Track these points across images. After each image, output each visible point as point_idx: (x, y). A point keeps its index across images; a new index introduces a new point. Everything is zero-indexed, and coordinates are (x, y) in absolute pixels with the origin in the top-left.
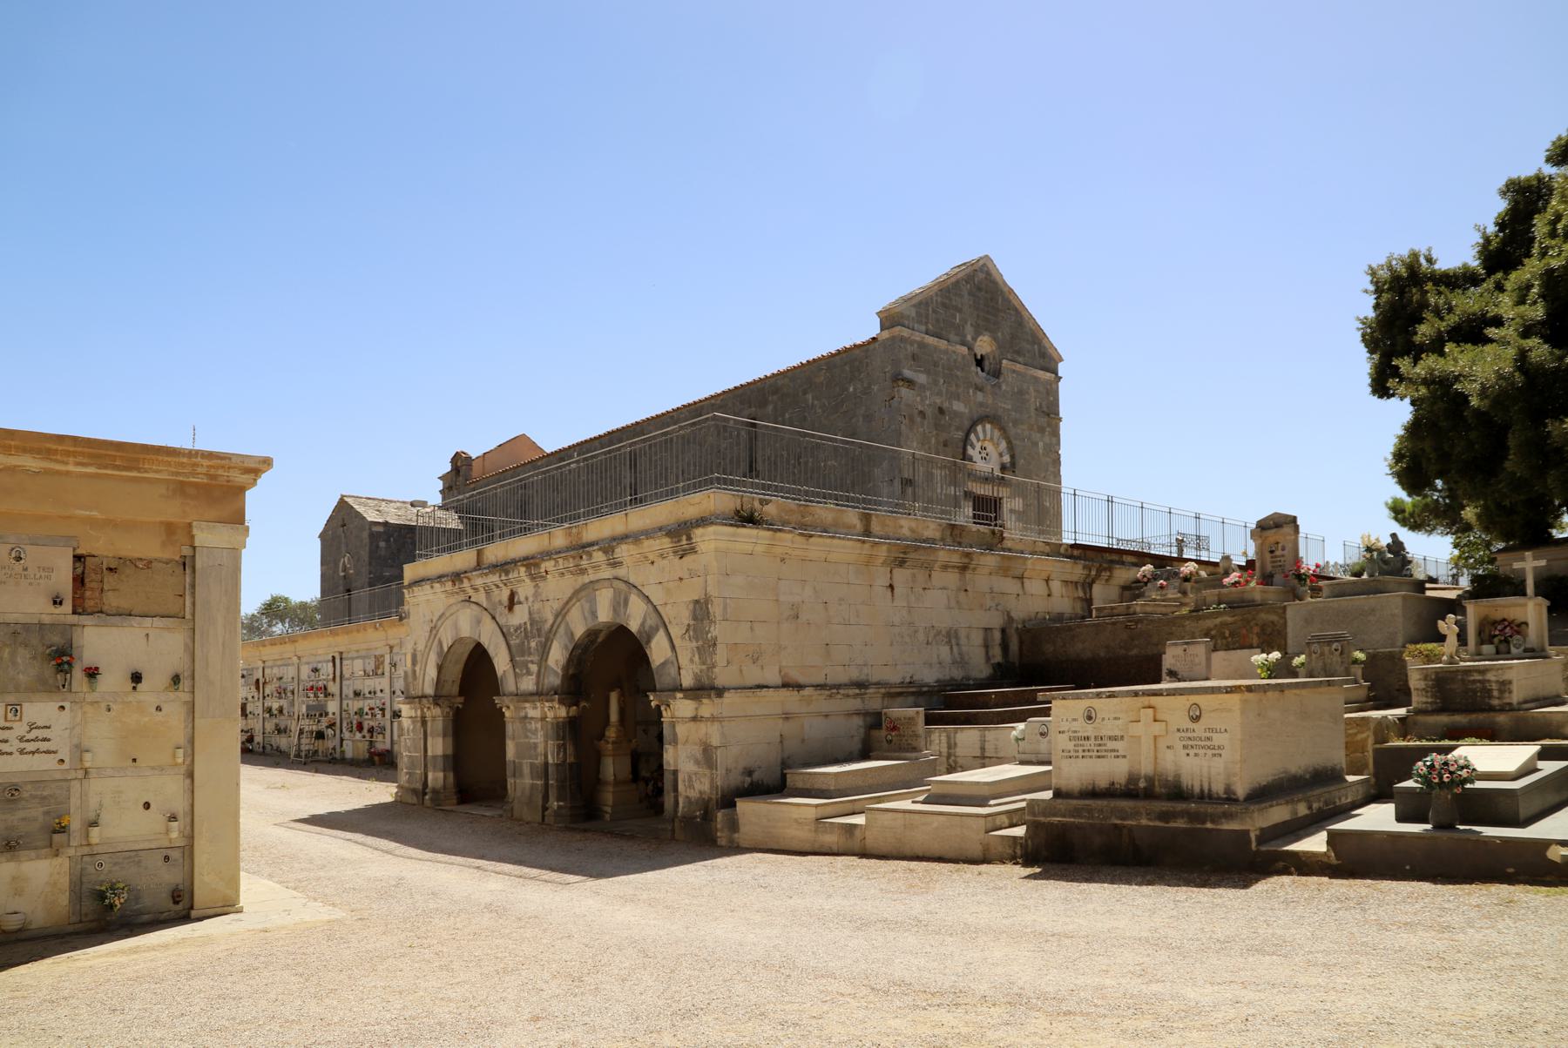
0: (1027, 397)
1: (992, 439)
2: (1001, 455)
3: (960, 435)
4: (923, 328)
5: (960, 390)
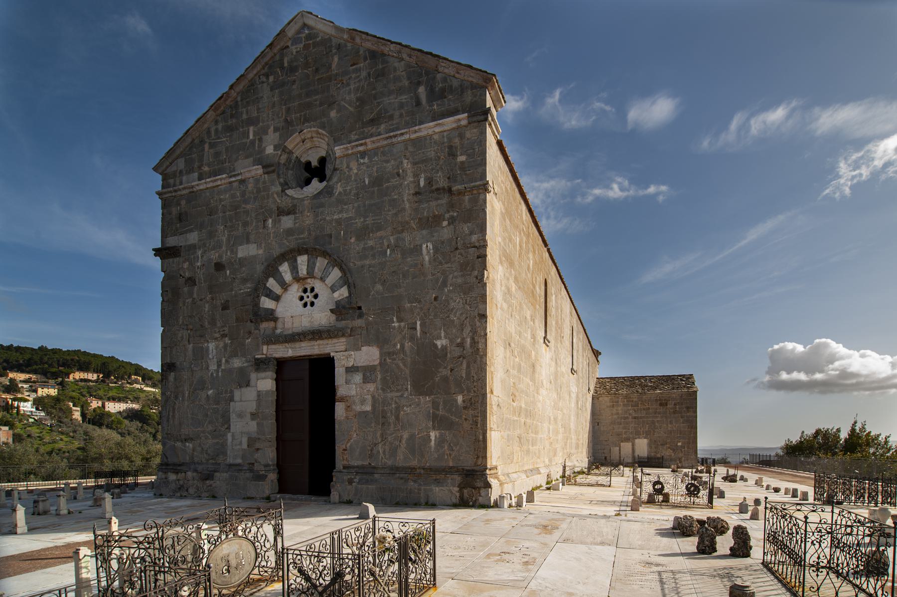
1: (311, 274)
3: (248, 287)
4: (196, 175)
5: (249, 229)
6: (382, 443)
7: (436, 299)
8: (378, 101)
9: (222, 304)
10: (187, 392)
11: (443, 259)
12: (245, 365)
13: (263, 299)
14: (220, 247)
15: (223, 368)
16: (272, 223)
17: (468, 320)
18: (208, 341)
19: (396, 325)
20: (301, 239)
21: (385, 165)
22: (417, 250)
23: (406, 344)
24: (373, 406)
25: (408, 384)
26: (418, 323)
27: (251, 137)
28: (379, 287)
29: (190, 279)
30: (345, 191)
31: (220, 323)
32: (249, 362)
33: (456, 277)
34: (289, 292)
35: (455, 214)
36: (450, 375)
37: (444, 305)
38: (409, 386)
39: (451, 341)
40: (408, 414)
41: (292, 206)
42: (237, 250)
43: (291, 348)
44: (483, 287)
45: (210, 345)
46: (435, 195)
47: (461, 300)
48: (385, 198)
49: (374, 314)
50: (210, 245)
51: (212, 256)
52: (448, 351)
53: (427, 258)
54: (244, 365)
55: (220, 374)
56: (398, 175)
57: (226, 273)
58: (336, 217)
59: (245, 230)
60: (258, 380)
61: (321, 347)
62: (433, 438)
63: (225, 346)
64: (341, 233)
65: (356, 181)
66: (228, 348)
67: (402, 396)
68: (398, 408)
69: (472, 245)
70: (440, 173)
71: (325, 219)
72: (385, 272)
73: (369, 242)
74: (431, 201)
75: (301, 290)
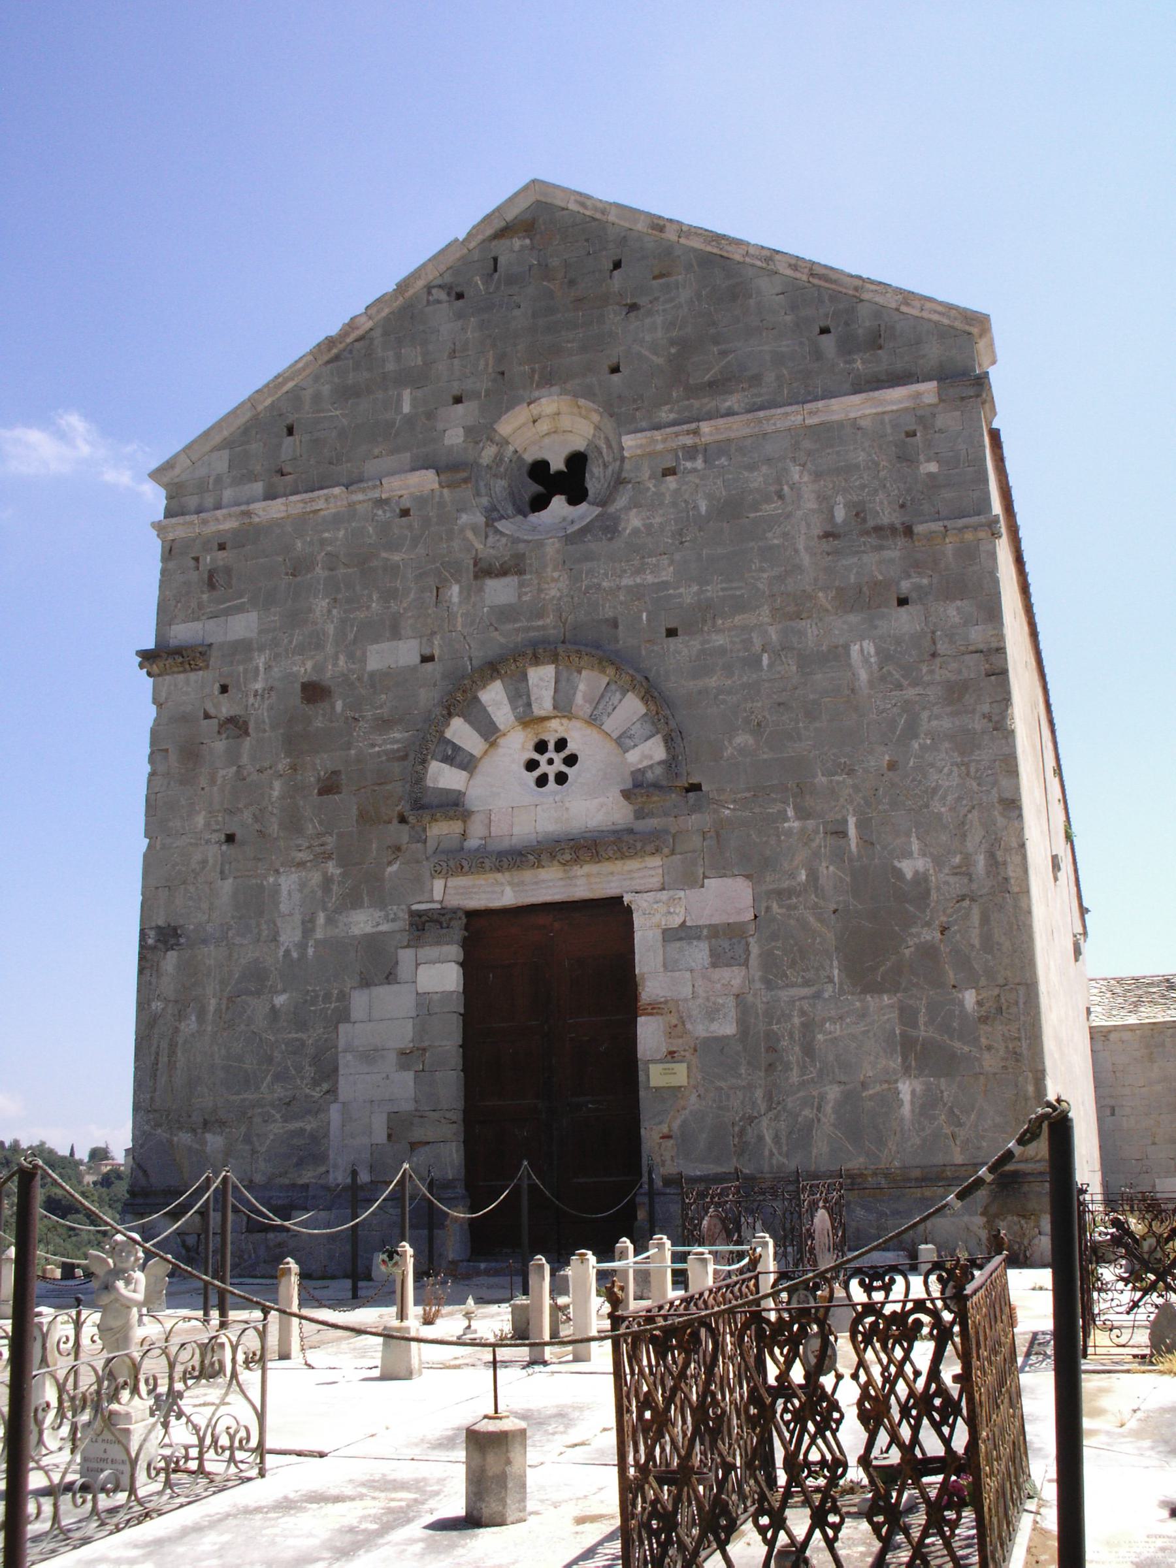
0: (771, 508)
1: (563, 708)
2: (623, 742)
6: (771, 1114)
7: (892, 766)
8: (723, 347)
9: (319, 780)
10: (213, 1002)
11: (903, 676)
12: (384, 928)
13: (435, 766)
14: (319, 646)
15: (319, 934)
16: (461, 592)
17: (975, 813)
18: (277, 871)
19: (796, 824)
20: (538, 628)
21: (746, 474)
22: (837, 655)
23: (822, 870)
24: (743, 1023)
25: (831, 967)
26: (852, 821)
27: (406, 408)
28: (743, 739)
29: (231, 720)
30: (649, 527)
31: (315, 827)
32: (393, 920)
33: (938, 717)
34: (501, 751)
35: (925, 581)
36: (941, 941)
37: (914, 780)
38: (836, 972)
39: (938, 862)
40: (836, 1038)
41: (512, 556)
42: (364, 654)
43: (510, 884)
44: (1006, 738)
45: (282, 880)
46: (873, 540)
47: (955, 769)
48: (752, 544)
49: (734, 802)
50: (291, 642)
51: (295, 669)
52: (933, 885)
53: (863, 675)
55: (310, 951)
56: (781, 496)
57: (333, 707)
58: (626, 581)
59: (389, 608)
60: (417, 965)
62: (906, 1096)
63: (327, 881)
64: (640, 618)
65: (674, 504)
66: (335, 887)
67: (817, 996)
68: (808, 1027)
69: (971, 648)
70: (881, 496)
71: (598, 587)
72: (759, 704)
73: (714, 637)
74: (864, 552)
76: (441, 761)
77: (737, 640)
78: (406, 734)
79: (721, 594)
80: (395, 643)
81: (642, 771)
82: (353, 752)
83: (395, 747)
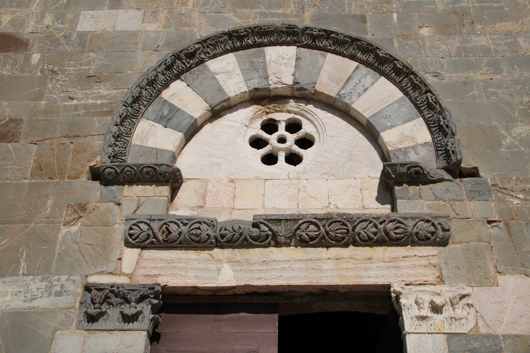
12: (42, 303)
20: (274, 15)
32: (59, 294)
54: (35, 303)
57: (28, 59)
61: (344, 265)
75: (258, 123)
76: (153, 121)
77: (502, 43)
78: (115, 91)
79: (477, 4)
80: (114, 12)
81: (405, 151)
82: (43, 103)
83: (99, 102)
